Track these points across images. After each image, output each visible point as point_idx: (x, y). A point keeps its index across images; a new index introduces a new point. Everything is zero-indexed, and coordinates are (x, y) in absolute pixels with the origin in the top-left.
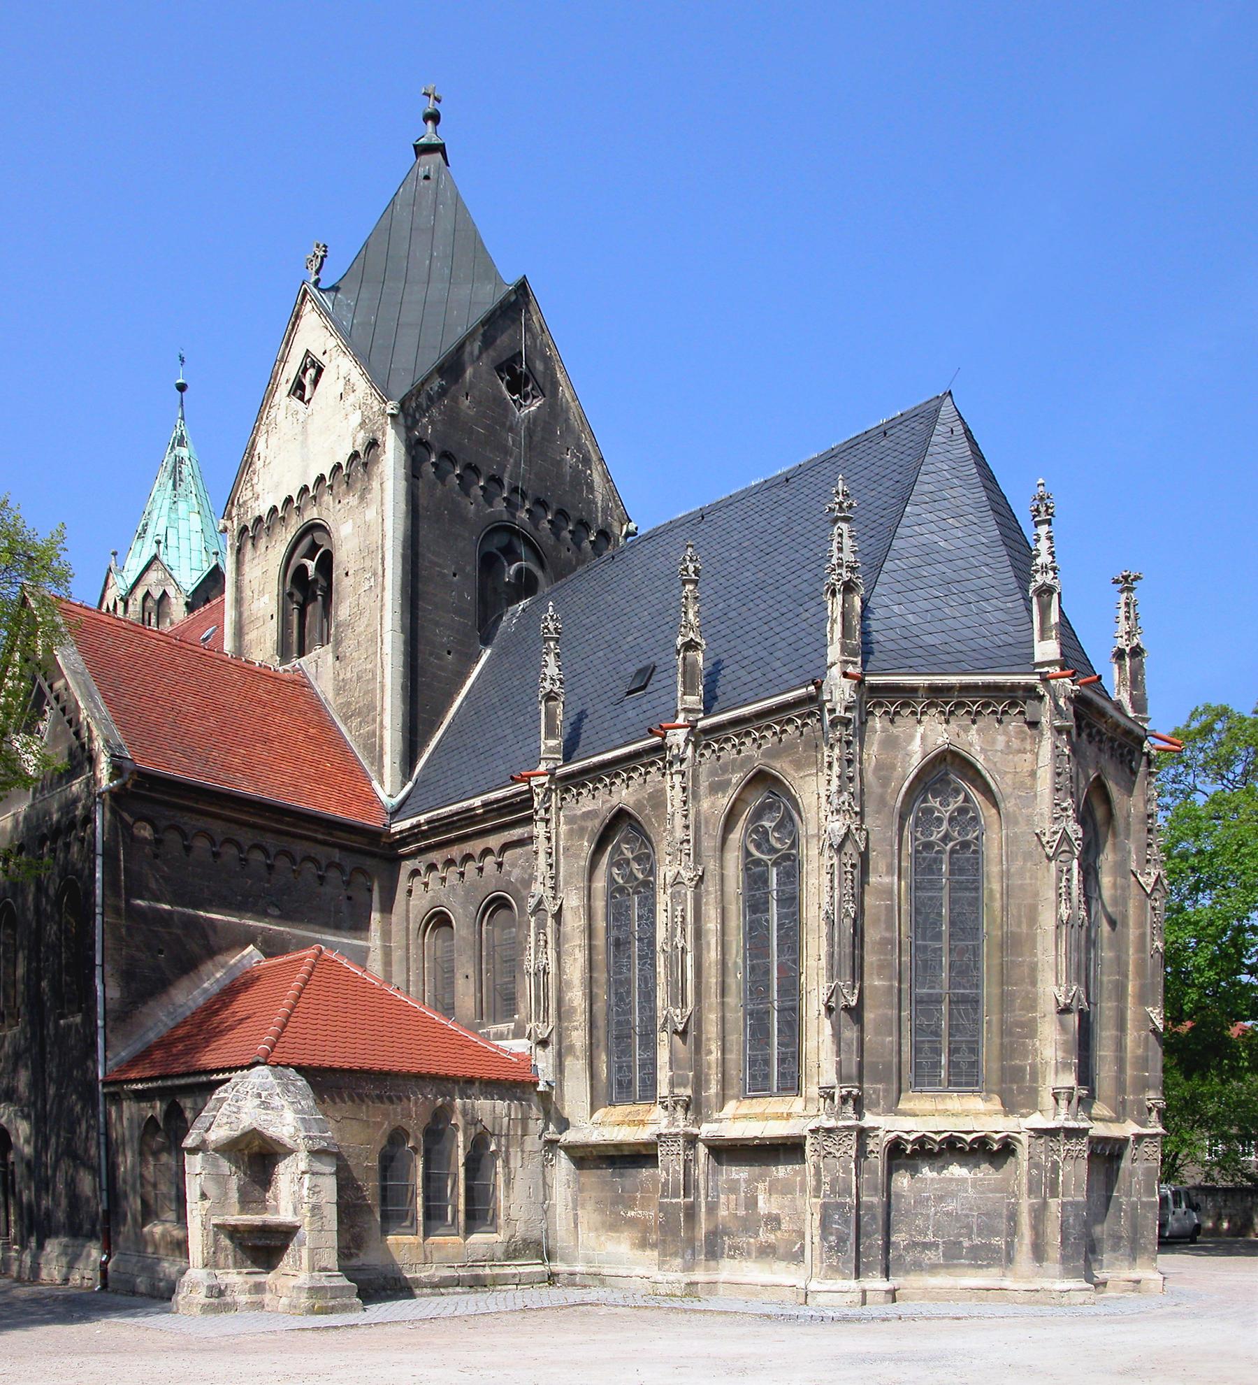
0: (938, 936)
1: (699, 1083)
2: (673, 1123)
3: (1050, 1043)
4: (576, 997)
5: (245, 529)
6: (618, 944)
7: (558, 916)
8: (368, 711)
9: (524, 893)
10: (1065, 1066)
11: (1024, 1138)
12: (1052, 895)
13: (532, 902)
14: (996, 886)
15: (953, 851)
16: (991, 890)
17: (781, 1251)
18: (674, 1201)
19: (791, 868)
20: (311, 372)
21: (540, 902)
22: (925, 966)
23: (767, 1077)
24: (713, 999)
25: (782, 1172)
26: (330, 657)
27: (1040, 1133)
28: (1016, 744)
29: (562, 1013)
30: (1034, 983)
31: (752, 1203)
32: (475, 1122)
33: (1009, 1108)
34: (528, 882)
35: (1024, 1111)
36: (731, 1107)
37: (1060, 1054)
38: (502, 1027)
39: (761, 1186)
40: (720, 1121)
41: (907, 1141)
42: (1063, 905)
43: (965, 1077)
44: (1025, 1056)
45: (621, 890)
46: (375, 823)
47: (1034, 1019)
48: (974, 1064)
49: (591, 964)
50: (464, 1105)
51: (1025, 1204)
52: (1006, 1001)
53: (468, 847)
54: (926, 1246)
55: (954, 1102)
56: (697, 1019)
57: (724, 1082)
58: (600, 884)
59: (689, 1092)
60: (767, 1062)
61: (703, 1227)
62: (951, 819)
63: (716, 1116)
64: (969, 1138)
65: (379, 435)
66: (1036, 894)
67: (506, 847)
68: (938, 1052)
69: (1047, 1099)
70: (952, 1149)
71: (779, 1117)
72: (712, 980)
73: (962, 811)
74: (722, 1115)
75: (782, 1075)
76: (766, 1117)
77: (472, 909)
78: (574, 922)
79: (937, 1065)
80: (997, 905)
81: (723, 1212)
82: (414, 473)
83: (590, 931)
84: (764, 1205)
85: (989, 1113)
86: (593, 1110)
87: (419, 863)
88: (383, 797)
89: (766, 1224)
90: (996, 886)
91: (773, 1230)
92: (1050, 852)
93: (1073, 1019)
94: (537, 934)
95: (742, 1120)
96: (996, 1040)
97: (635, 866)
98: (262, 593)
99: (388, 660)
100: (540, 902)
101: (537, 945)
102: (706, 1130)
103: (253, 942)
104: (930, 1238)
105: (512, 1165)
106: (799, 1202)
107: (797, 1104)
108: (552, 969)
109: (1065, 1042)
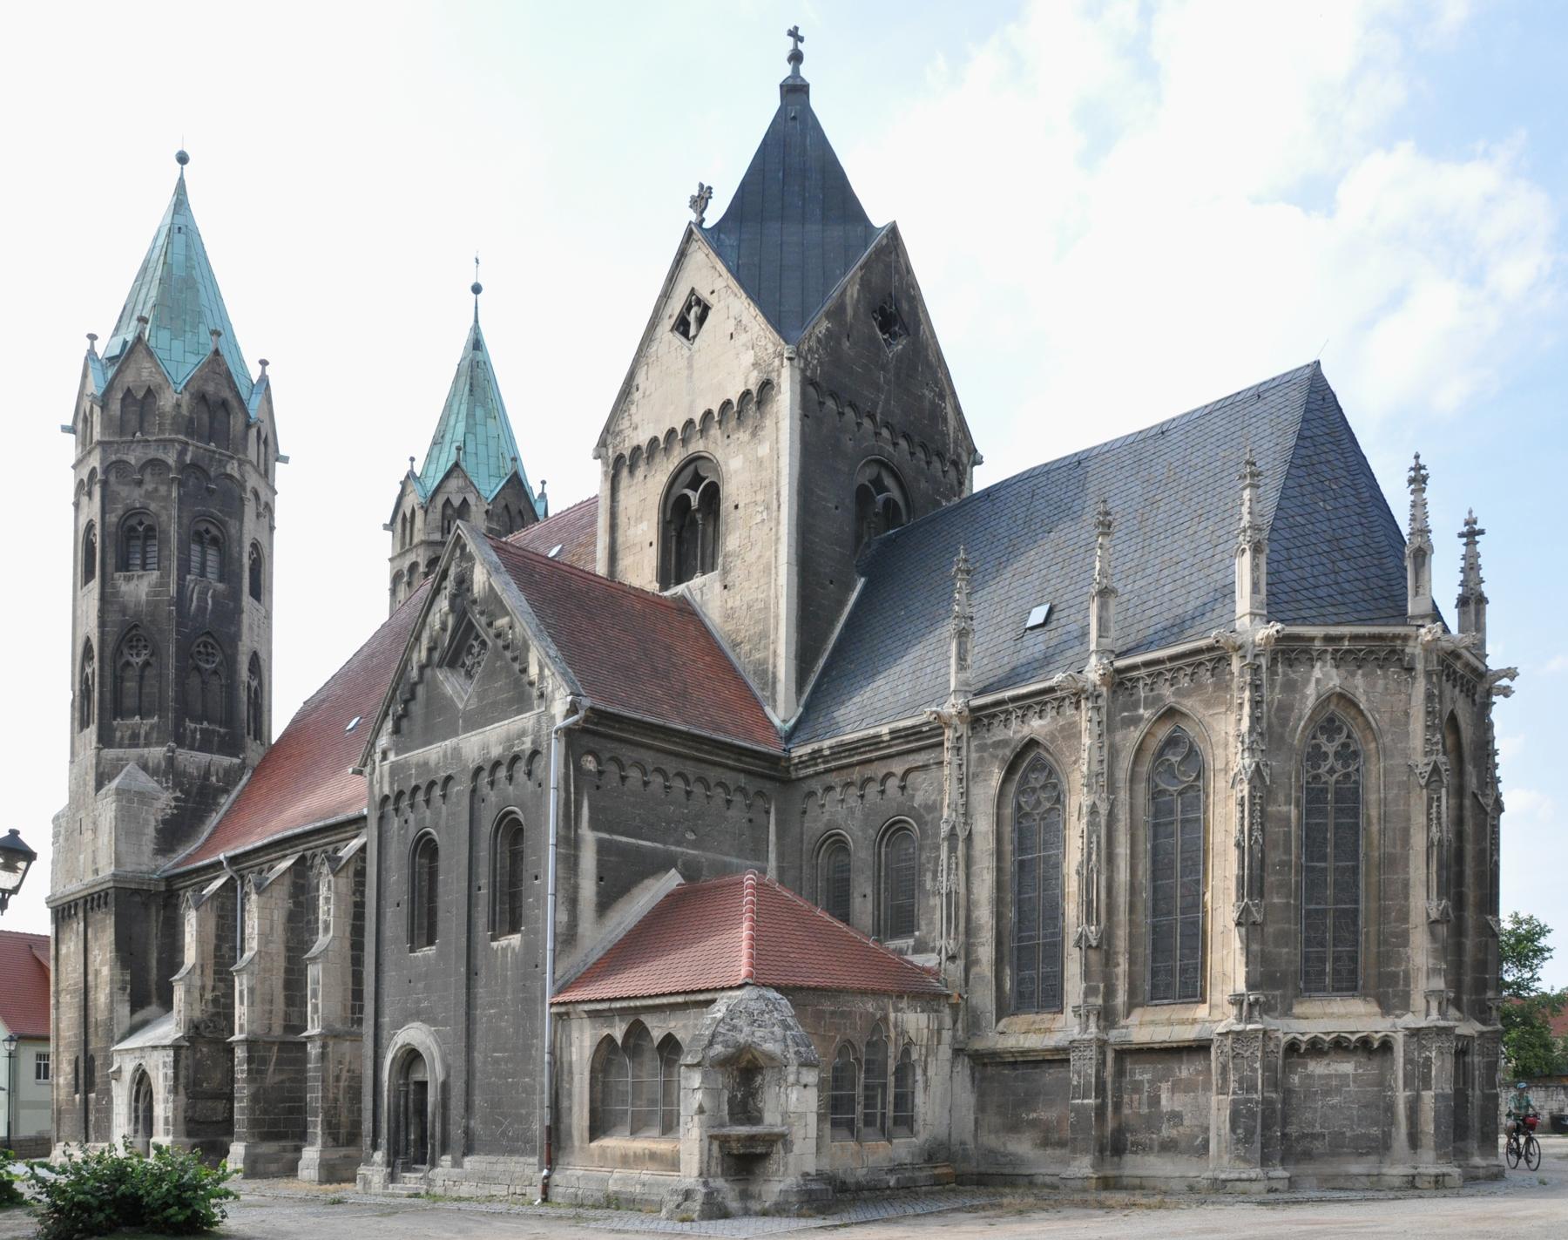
3: (1420, 953)
5: (620, 457)
6: (1022, 864)
9: (929, 818)
12: (1423, 819)
15: (1337, 782)
16: (1369, 816)
17: (1183, 1145)
19: (1195, 795)
20: (695, 311)
22: (1314, 879)
23: (1169, 986)
26: (718, 586)
27: (1414, 1033)
28: (1392, 685)
29: (970, 931)
30: (1407, 898)
33: (1386, 1009)
34: (934, 808)
37: (1431, 961)
42: (1434, 829)
43: (1347, 984)
44: (1399, 964)
45: (1027, 814)
47: (1406, 932)
48: (1354, 972)
49: (999, 885)
51: (1401, 1096)
52: (1383, 912)
53: (869, 771)
54: (1314, 1136)
58: (1008, 811)
62: (1336, 753)
64: (1353, 1038)
65: (774, 375)
66: (1409, 819)
68: (1323, 961)
69: (1418, 1001)
70: (1340, 1046)
71: (1183, 1022)
73: (1345, 746)
75: (1184, 984)
76: (1170, 1023)
77: (871, 832)
79: (1323, 972)
82: (809, 413)
83: (999, 854)
85: (1369, 1015)
88: (777, 722)
90: (1374, 813)
91: (1175, 1126)
92: (1423, 782)
93: (1443, 930)
95: (1150, 1026)
96: (1374, 949)
98: (639, 519)
99: (783, 592)
104: (1318, 1129)
106: (1201, 1100)
109: (1436, 950)
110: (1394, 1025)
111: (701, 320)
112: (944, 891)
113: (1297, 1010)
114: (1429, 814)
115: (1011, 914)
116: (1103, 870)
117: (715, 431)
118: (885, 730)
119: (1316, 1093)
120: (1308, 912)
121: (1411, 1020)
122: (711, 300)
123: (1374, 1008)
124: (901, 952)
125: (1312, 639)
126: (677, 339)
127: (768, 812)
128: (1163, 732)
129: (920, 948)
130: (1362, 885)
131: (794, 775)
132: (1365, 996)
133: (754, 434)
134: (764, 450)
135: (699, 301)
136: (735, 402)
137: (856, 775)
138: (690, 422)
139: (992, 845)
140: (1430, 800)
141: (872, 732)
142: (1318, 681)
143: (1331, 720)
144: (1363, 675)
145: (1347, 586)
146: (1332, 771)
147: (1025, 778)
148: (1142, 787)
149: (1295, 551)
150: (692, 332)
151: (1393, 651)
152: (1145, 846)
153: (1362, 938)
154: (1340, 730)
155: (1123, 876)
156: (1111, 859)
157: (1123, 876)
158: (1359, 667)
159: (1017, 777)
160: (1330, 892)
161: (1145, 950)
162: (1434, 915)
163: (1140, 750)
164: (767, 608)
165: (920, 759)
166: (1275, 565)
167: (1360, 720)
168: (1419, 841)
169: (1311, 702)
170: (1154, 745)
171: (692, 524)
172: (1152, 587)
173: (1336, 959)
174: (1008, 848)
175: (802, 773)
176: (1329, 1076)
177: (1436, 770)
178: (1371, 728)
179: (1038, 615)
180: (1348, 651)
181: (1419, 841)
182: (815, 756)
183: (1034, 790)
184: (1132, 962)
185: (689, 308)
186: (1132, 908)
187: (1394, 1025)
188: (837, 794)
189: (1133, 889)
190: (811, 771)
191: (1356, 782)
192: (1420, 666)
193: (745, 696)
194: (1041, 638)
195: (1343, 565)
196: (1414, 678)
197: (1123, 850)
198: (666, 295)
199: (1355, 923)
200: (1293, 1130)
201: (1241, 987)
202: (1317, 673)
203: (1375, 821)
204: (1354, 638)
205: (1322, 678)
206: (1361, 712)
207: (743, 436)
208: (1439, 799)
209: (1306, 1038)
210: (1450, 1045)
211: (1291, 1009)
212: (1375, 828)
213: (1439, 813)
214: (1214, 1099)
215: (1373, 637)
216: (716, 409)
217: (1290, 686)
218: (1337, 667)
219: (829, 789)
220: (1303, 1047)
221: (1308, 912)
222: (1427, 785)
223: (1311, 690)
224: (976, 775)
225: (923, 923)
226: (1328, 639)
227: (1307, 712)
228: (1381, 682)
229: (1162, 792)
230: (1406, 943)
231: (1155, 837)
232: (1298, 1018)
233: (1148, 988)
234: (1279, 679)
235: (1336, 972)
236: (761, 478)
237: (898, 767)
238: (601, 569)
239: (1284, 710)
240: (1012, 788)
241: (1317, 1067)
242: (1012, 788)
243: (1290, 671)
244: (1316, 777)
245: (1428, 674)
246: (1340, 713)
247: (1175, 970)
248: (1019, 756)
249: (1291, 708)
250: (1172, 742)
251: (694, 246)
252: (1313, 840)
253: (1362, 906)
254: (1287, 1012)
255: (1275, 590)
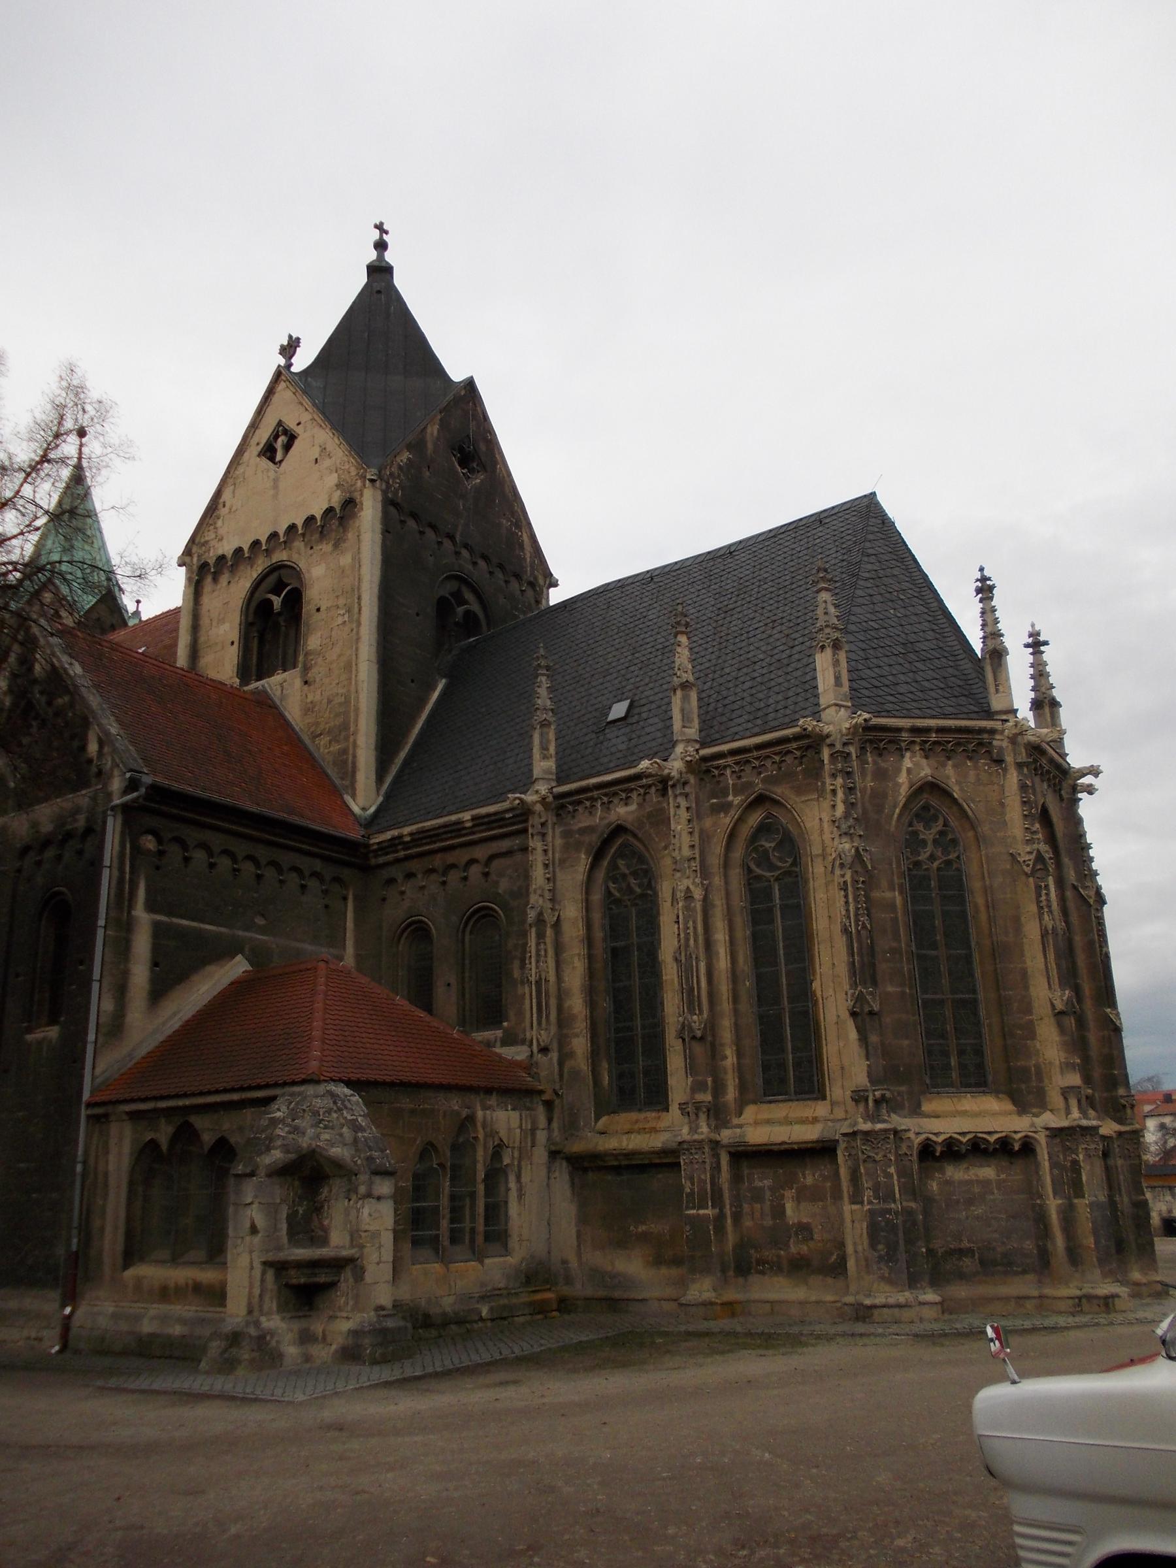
0: (934, 945)
1: (719, 1089)
2: (694, 1129)
3: (1050, 1046)
4: (577, 1004)
6: (615, 952)
7: (557, 925)
8: (343, 731)
10: (1067, 1067)
11: (1042, 1138)
12: (1033, 908)
13: (532, 915)
14: (980, 901)
15: (939, 869)
16: (976, 906)
18: (701, 1212)
20: (282, 440)
21: (541, 914)
23: (783, 1081)
24: (726, 1006)
25: (809, 1177)
27: (1055, 1133)
29: (564, 1020)
30: (1026, 988)
31: (779, 1211)
32: (492, 1134)
33: (1022, 1107)
34: (523, 893)
35: (1034, 1110)
36: (750, 1112)
37: (1063, 1055)
38: (488, 1034)
39: (789, 1194)
40: (740, 1126)
41: (935, 1142)
42: (1046, 917)
43: (976, 1080)
45: (618, 902)
46: (355, 834)
47: (1031, 1021)
49: (591, 973)
50: (484, 1117)
53: (451, 858)
55: (969, 1103)
56: (712, 1026)
57: (742, 1087)
58: (597, 897)
59: (707, 1097)
60: (782, 1066)
61: (731, 1238)
62: (935, 841)
63: (735, 1121)
64: (992, 1139)
66: (1018, 907)
67: (492, 858)
68: (946, 1054)
70: (978, 1149)
71: (803, 1121)
72: (724, 988)
74: (742, 1120)
76: (787, 1121)
78: (573, 931)
79: (947, 1067)
80: (983, 917)
81: (748, 1223)
83: (589, 940)
84: (792, 1212)
86: (597, 1119)
87: (397, 872)
88: (356, 809)
89: (797, 1234)
90: (980, 901)
92: (1028, 870)
93: (1070, 1022)
94: (538, 944)
95: (769, 1124)
97: (632, 881)
100: (541, 914)
101: (538, 955)
102: (726, 1136)
103: (242, 952)
105: (523, 1180)
107: (821, 1109)
108: (552, 978)
110: (1033, 1125)
111: (288, 447)
112: (533, 979)
113: (926, 1107)
114: (1038, 902)
115: (605, 1004)
116: (702, 956)
117: (298, 544)
118: (467, 816)
119: (958, 1202)
120: (926, 1003)
121: (1050, 1119)
122: (298, 430)
123: (1009, 1106)
124: (489, 1044)
125: (899, 730)
126: (265, 463)
127: (345, 899)
128: (755, 818)
129: (510, 1040)
130: (978, 973)
131: (373, 862)
132: (996, 1092)
133: (336, 546)
134: (346, 560)
135: (285, 432)
136: (318, 517)
137: (437, 861)
138: (274, 535)
139: (582, 932)
140: (1038, 888)
141: (453, 818)
142: (909, 771)
143: (926, 808)
144: (954, 766)
145: (926, 684)
146: (932, 858)
147: (613, 866)
148: (736, 874)
149: (871, 652)
150: (279, 457)
151: (981, 744)
152: (743, 932)
153: (985, 1030)
154: (935, 818)
155: (723, 963)
156: (709, 945)
157: (723, 963)
158: (949, 758)
159: (605, 863)
160: (945, 982)
161: (752, 1042)
162: (1060, 1006)
163: (732, 836)
164: (347, 702)
165: (505, 845)
166: (853, 663)
167: (955, 808)
168: (1032, 931)
169: (904, 791)
170: (746, 831)
171: (276, 623)
172: (731, 685)
173: (961, 1053)
174: (598, 934)
175: (381, 860)
176: (969, 1183)
177: (1040, 858)
178: (967, 817)
179: (619, 710)
180: (935, 743)
181: (1032, 931)
182: (395, 843)
183: (624, 876)
184: (739, 1054)
185: (276, 437)
186: (735, 999)
187: (1033, 1125)
188: (420, 881)
189: (734, 977)
190: (390, 857)
191: (958, 870)
192: (1009, 759)
193: (331, 786)
194: (623, 731)
195: (920, 665)
196: (1005, 770)
197: (720, 936)
198: (254, 426)
199: (975, 1013)
200: (938, 1245)
201: (859, 1076)
202: (907, 763)
203: (982, 909)
204: (941, 730)
205: (912, 768)
206: (955, 801)
207: (326, 547)
208: (1047, 887)
209: (940, 1139)
210: (1098, 1146)
211: (919, 1105)
212: (983, 917)
213: (1048, 900)
214: (847, 1208)
215: (959, 730)
216: (299, 523)
217: (882, 775)
218: (926, 757)
219: (410, 875)
220: (939, 1149)
221: (925, 1002)
222: (1033, 874)
223: (903, 778)
224: (562, 861)
225: (511, 1014)
226: (915, 730)
227: (902, 800)
228: (972, 773)
229: (758, 878)
230: (1032, 1035)
231: (755, 922)
232: (929, 1116)
233: (760, 1081)
234: (870, 767)
235: (962, 1067)
236: (345, 587)
237: (481, 853)
238: (182, 660)
239: (879, 798)
240: (600, 875)
241: (956, 1173)
242: (600, 875)
243: (879, 760)
244: (917, 864)
245: (1019, 766)
246: (934, 802)
247: (788, 1064)
248: (606, 842)
249: (885, 796)
250: (763, 829)
251: (282, 385)
252: (921, 927)
253: (981, 996)
254: (916, 1111)
255: (855, 686)
